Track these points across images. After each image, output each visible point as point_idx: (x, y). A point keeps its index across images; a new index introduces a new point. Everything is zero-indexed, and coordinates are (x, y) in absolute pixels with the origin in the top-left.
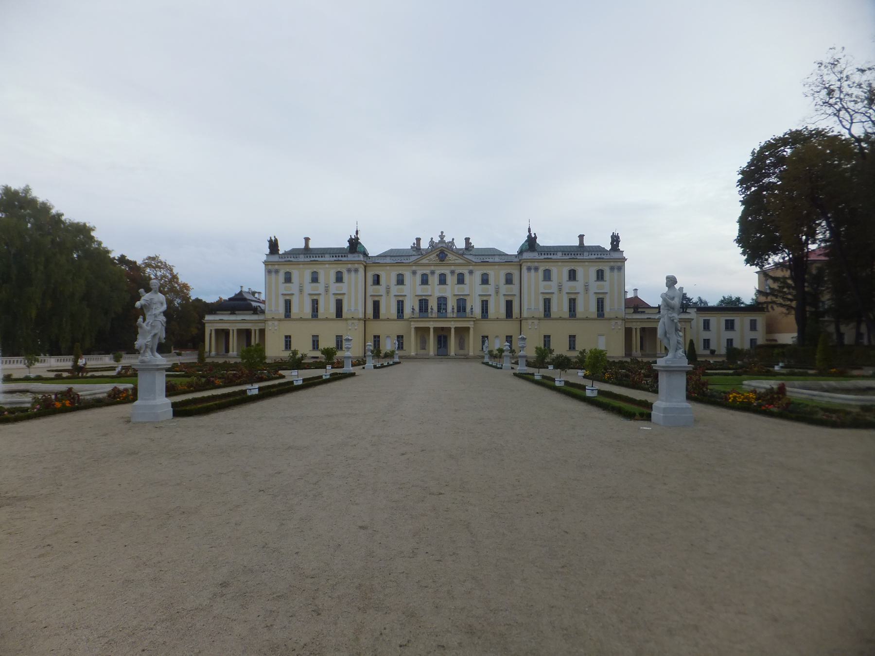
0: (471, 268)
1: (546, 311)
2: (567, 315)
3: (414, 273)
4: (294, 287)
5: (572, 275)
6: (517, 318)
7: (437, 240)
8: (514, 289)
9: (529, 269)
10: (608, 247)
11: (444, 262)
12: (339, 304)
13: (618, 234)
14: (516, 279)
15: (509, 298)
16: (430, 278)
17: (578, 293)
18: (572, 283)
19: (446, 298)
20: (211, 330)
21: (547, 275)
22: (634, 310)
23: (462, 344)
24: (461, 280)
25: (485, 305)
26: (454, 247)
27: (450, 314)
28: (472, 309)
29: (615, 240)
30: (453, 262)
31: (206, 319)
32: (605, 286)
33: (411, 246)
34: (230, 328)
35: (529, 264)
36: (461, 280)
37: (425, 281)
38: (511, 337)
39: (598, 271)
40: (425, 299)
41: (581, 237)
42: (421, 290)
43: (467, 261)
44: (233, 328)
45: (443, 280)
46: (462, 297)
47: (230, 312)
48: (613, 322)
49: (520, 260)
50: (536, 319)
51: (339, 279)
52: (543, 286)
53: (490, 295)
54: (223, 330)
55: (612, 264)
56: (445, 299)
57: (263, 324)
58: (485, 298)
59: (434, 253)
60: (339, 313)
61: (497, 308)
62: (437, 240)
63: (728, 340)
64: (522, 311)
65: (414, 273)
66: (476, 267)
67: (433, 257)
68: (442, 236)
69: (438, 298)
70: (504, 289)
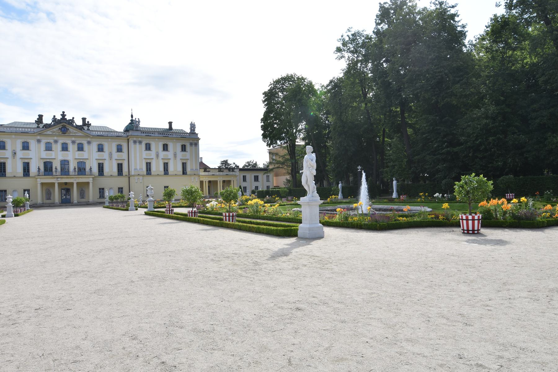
0: (89, 139)
1: (148, 170)
2: (163, 173)
3: (39, 141)
5: (165, 147)
6: (126, 175)
7: (59, 117)
8: (124, 155)
10: (188, 131)
11: (66, 134)
13: (194, 123)
14: (125, 149)
15: (120, 162)
16: (54, 146)
17: (170, 159)
18: (165, 153)
21: (148, 147)
23: (82, 194)
24: (80, 148)
25: (101, 167)
26: (75, 124)
27: (71, 173)
28: (91, 169)
29: (193, 126)
30: (74, 134)
32: (187, 155)
33: (36, 121)
35: (135, 139)
36: (80, 148)
37: (49, 148)
38: (122, 188)
39: (182, 146)
41: (170, 123)
42: (45, 155)
43: (85, 135)
45: (65, 148)
46: (81, 161)
48: (192, 177)
50: (141, 175)
52: (145, 154)
56: (68, 162)
58: (101, 162)
59: (58, 127)
61: (110, 168)
62: (59, 117)
64: (130, 170)
65: (39, 141)
66: (93, 140)
67: (56, 129)
68: (63, 115)
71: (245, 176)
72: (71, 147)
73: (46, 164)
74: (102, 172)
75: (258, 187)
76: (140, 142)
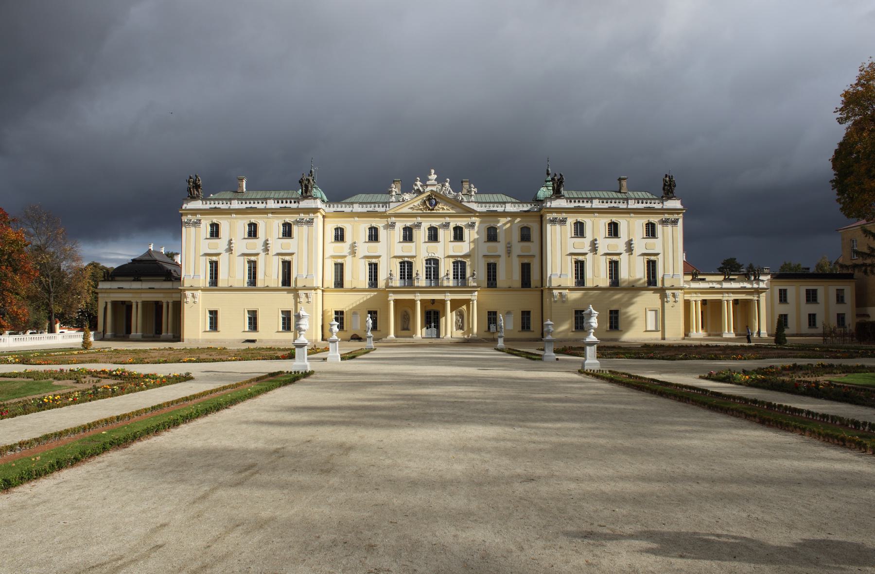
3: (392, 226)
4: (220, 245)
5: (614, 230)
6: (536, 287)
8: (533, 247)
9: (553, 221)
12: (287, 267)
14: (535, 235)
15: (526, 261)
19: (438, 260)
20: (106, 303)
21: (579, 230)
22: (693, 277)
31: (98, 287)
34: (133, 301)
37: (408, 235)
39: (647, 225)
40: (408, 262)
44: (136, 299)
45: (433, 236)
47: (132, 279)
49: (540, 210)
51: (287, 232)
53: (499, 256)
54: (123, 302)
55: (667, 216)
56: (436, 262)
57: (179, 295)
58: (492, 261)
60: (287, 280)
63: (810, 315)
64: (544, 277)
69: (426, 260)
70: (518, 248)
71: (785, 290)
72: (441, 232)
73: (402, 264)
74: (493, 280)
75: (814, 315)
76: (563, 222)
